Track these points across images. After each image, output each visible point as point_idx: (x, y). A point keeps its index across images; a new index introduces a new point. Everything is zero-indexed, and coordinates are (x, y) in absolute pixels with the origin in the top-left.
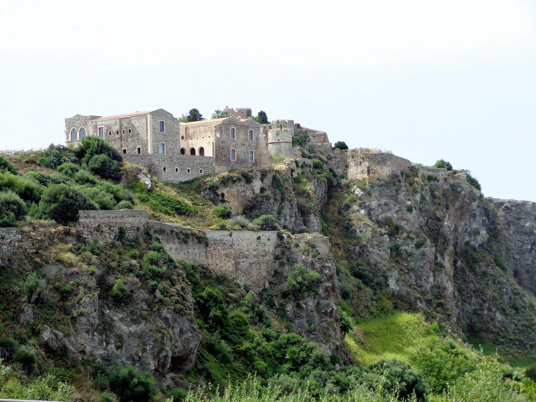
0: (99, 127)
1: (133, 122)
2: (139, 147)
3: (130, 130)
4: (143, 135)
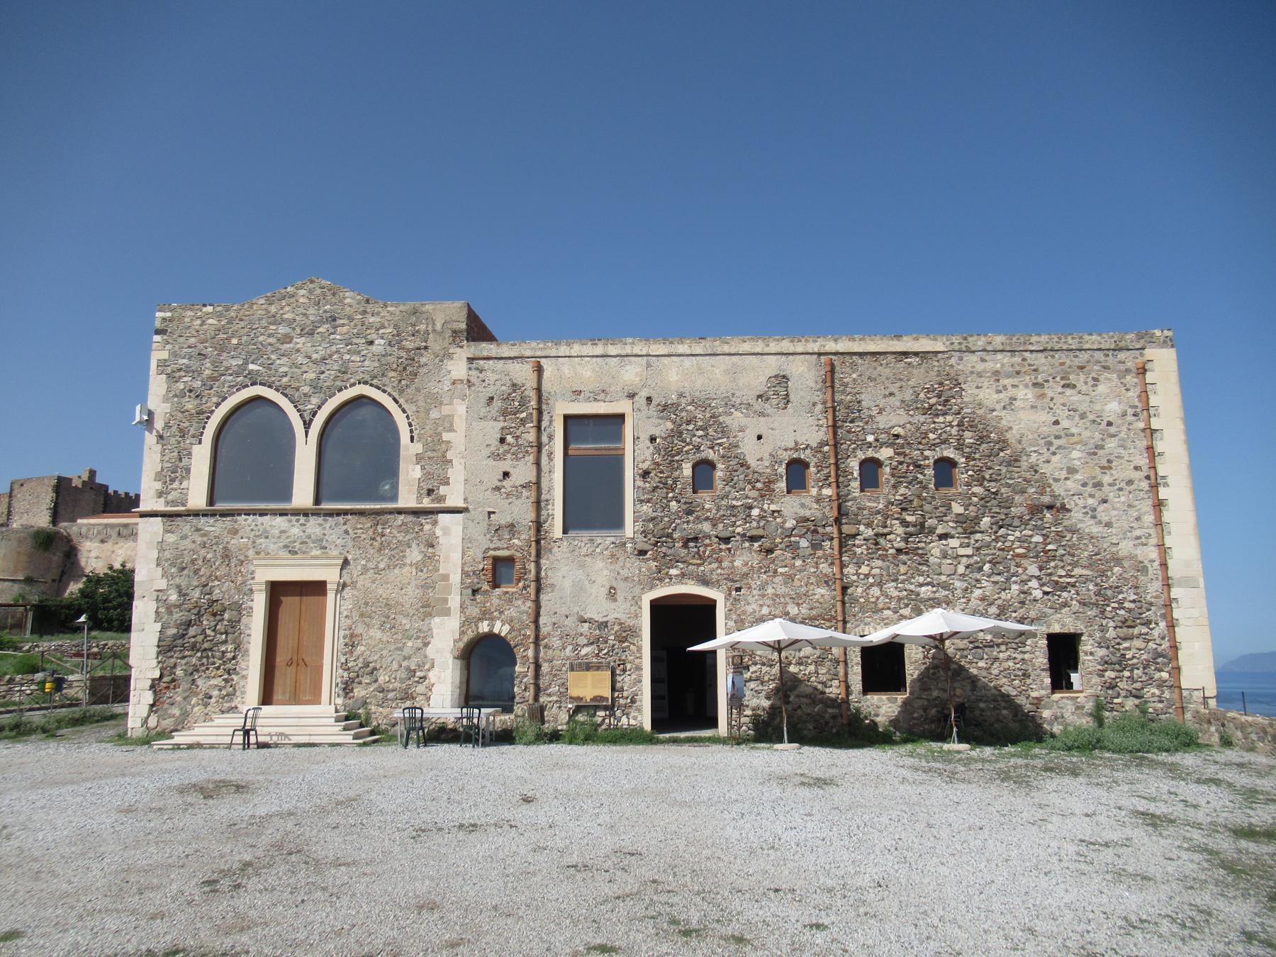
0: (561, 408)
1: (981, 395)
2: (1061, 623)
3: (945, 469)
4: (1109, 523)
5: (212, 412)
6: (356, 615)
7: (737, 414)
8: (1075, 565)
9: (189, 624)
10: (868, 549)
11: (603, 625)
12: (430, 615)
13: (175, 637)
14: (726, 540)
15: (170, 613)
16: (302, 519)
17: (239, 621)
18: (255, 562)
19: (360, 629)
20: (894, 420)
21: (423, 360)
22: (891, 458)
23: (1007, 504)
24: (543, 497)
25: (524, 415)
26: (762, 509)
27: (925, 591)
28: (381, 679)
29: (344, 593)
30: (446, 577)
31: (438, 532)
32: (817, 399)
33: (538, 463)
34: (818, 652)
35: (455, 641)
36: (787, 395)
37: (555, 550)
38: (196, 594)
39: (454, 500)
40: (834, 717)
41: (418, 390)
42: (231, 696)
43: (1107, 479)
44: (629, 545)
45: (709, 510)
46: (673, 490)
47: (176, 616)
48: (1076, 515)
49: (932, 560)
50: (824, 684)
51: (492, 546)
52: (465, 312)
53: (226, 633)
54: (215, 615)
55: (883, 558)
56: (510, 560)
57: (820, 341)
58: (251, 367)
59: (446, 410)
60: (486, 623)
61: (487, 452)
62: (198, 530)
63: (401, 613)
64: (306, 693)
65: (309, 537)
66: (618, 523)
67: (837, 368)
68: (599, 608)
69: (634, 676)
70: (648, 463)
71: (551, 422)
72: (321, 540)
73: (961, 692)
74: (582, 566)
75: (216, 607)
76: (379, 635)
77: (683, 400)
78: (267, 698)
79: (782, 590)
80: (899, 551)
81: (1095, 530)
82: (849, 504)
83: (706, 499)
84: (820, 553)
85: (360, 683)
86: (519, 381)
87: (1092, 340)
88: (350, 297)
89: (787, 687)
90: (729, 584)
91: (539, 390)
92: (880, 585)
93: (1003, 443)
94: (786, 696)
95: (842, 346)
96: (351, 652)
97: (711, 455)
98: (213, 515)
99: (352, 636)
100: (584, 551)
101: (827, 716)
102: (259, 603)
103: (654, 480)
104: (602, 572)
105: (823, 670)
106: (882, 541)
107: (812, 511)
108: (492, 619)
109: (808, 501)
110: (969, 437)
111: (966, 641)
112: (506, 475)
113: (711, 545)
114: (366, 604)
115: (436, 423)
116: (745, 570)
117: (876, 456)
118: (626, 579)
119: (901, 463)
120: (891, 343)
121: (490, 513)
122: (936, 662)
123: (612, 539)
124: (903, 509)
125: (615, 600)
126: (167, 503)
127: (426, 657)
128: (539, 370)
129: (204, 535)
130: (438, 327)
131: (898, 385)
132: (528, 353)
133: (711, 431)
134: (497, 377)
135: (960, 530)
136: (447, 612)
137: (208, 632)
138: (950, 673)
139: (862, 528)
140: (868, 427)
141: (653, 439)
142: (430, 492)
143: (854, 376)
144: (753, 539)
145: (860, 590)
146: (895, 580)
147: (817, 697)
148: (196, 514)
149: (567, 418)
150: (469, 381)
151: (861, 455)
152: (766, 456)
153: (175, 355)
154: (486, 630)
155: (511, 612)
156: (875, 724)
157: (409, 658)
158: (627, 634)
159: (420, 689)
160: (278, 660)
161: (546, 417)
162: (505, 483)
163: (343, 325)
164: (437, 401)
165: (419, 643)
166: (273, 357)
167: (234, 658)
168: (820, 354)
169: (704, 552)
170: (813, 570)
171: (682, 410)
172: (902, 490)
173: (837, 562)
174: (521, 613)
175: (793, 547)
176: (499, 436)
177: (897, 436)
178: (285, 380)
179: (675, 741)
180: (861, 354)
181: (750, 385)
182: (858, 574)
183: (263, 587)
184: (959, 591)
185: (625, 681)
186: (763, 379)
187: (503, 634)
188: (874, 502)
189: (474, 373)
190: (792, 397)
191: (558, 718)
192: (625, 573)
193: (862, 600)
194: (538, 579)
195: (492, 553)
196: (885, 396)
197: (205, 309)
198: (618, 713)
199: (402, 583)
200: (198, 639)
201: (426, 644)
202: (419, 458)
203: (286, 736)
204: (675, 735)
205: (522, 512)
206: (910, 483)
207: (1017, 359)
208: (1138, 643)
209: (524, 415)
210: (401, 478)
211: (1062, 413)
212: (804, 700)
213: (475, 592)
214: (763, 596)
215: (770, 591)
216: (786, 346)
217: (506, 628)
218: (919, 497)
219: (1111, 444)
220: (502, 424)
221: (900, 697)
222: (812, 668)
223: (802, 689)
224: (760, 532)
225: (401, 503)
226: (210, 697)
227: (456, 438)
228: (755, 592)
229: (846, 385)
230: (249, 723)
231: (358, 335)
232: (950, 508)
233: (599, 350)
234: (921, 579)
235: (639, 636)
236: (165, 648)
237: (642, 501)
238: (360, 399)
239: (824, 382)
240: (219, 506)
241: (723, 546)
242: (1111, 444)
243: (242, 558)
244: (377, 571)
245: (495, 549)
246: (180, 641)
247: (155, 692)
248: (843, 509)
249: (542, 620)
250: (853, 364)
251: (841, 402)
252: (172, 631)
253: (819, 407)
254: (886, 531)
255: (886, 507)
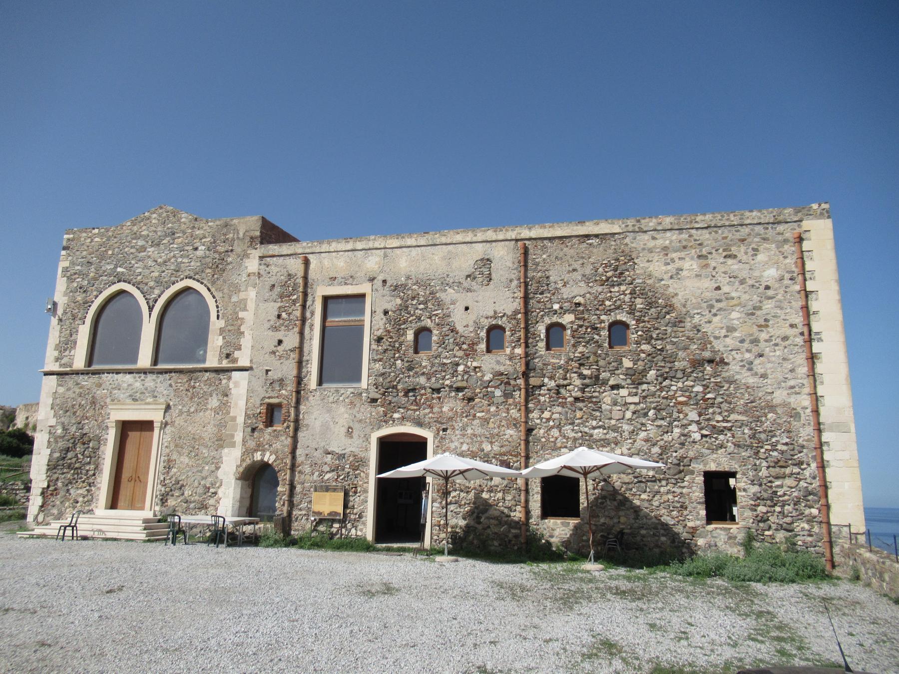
0: (321, 290)
1: (652, 267)
2: (717, 462)
3: (618, 331)
5: (92, 302)
6: (172, 446)
7: (450, 291)
8: (732, 411)
9: (68, 450)
10: (550, 397)
11: (342, 456)
12: (222, 447)
13: (58, 459)
14: (438, 391)
15: (57, 442)
16: (143, 376)
17: (99, 448)
18: (110, 407)
19: (174, 457)
20: (576, 290)
21: (230, 259)
22: (572, 322)
23: (672, 359)
24: (305, 358)
25: (295, 297)
26: (466, 366)
27: (598, 433)
28: (186, 493)
29: (166, 430)
30: (234, 419)
31: (231, 385)
32: (513, 276)
33: (301, 333)
34: (505, 482)
35: (237, 466)
36: (490, 274)
37: (311, 398)
38: (73, 429)
39: (243, 362)
40: (516, 536)
41: (225, 281)
42: (90, 502)
43: (763, 336)
44: (364, 395)
45: (425, 367)
46: (399, 352)
47: (60, 444)
48: (734, 369)
49: (604, 407)
50: (510, 508)
51: (267, 395)
52: (259, 224)
53: (90, 457)
54: (84, 444)
55: (563, 405)
56: (279, 406)
57: (518, 230)
58: (119, 269)
59: (242, 295)
60: (259, 453)
61: (267, 325)
62: (77, 384)
63: (203, 445)
64: (135, 504)
65: (146, 389)
66: (359, 379)
67: (531, 251)
68: (339, 443)
69: (362, 497)
70: (381, 331)
71: (313, 301)
72: (154, 391)
73: (624, 521)
74: (329, 411)
75: (86, 439)
76: (186, 460)
77: (410, 282)
78: (113, 504)
79: (479, 431)
80: (577, 399)
81: (751, 381)
82: (536, 360)
83: (423, 359)
84: (510, 401)
85: (172, 495)
86: (292, 272)
87: (753, 216)
88: (185, 217)
89: (480, 510)
90: (438, 425)
91: (305, 277)
92: (559, 427)
93: (670, 308)
94: (478, 518)
95: (534, 233)
96: (168, 472)
97: (428, 323)
98: (88, 374)
99: (169, 461)
100: (331, 399)
101: (510, 536)
102: (111, 436)
103: (385, 344)
104: (343, 415)
105: (509, 497)
106: (562, 391)
107: (506, 366)
108: (264, 451)
109: (502, 359)
110: (639, 303)
111: (631, 476)
112: (280, 342)
113: (425, 394)
114: (180, 438)
115: (235, 304)
116: (450, 414)
117: (560, 321)
118: (360, 421)
119: (581, 326)
120: (575, 228)
121: (267, 371)
122: (604, 493)
123: (352, 390)
124: (581, 365)
125: (352, 437)
126: (61, 366)
127: (217, 478)
128: (307, 262)
129: (81, 388)
130: (241, 235)
131: (581, 262)
132: (300, 251)
133: (430, 305)
134: (278, 269)
135: (629, 381)
136: (233, 445)
137: (79, 456)
138: (616, 503)
139: (546, 380)
140: (554, 298)
141: (386, 313)
142: (228, 356)
143: (544, 256)
144: (459, 389)
145: (542, 431)
146: (572, 424)
147: (503, 520)
148: (77, 373)
149: (326, 299)
150: (259, 273)
151: (547, 321)
152: (471, 323)
153: (73, 263)
154: (259, 458)
155: (277, 445)
156: (549, 544)
157: (206, 478)
158: (359, 463)
159: (212, 502)
160: (123, 476)
161: (310, 298)
162: (279, 348)
163: (179, 237)
164: (237, 289)
165: (213, 467)
166: (133, 262)
167: (94, 475)
168: (517, 240)
169: (420, 400)
170: (504, 415)
171: (408, 290)
172: (581, 349)
173: (523, 408)
174: (284, 446)
175: (489, 396)
176: (277, 313)
177: (579, 304)
178: (139, 278)
179: (389, 550)
180: (550, 239)
181: (462, 268)
182: (541, 418)
183: (114, 424)
184: (626, 433)
185: (355, 500)
186: (472, 262)
187: (270, 462)
188: (557, 359)
189: (263, 267)
190: (493, 276)
191: (301, 526)
192: (360, 416)
193: (543, 440)
194: (297, 421)
195: (267, 401)
196: (569, 272)
197: (94, 231)
198: (349, 526)
199: (204, 423)
200: (72, 462)
201: (218, 468)
202: (222, 331)
203: (103, 532)
204: (389, 545)
205: (289, 370)
206: (587, 342)
207: (685, 236)
208: (789, 482)
209: (295, 297)
210: (209, 345)
211: (723, 280)
212: (492, 521)
213: (253, 430)
214: (463, 435)
215: (469, 431)
216: (490, 235)
217: (273, 457)
218: (595, 354)
219: (768, 306)
220: (279, 304)
221: (573, 522)
222: (500, 495)
223: (492, 512)
224: (464, 384)
225: (208, 365)
226: (77, 502)
227: (247, 316)
228: (457, 432)
229: (537, 264)
230: (74, 521)
231: (188, 244)
232: (621, 363)
233: (350, 246)
234: (594, 423)
235: (368, 466)
236: (52, 467)
237: (375, 361)
238: (188, 289)
239: (519, 262)
240: (95, 367)
241: (435, 396)
242: (768, 306)
243: (102, 404)
244: (189, 413)
245: (269, 398)
246: (61, 462)
247: (44, 497)
248: (531, 364)
249: (298, 452)
250: (544, 247)
251: (533, 278)
252: (57, 455)
253: (515, 283)
254: (565, 382)
255: (567, 362)
